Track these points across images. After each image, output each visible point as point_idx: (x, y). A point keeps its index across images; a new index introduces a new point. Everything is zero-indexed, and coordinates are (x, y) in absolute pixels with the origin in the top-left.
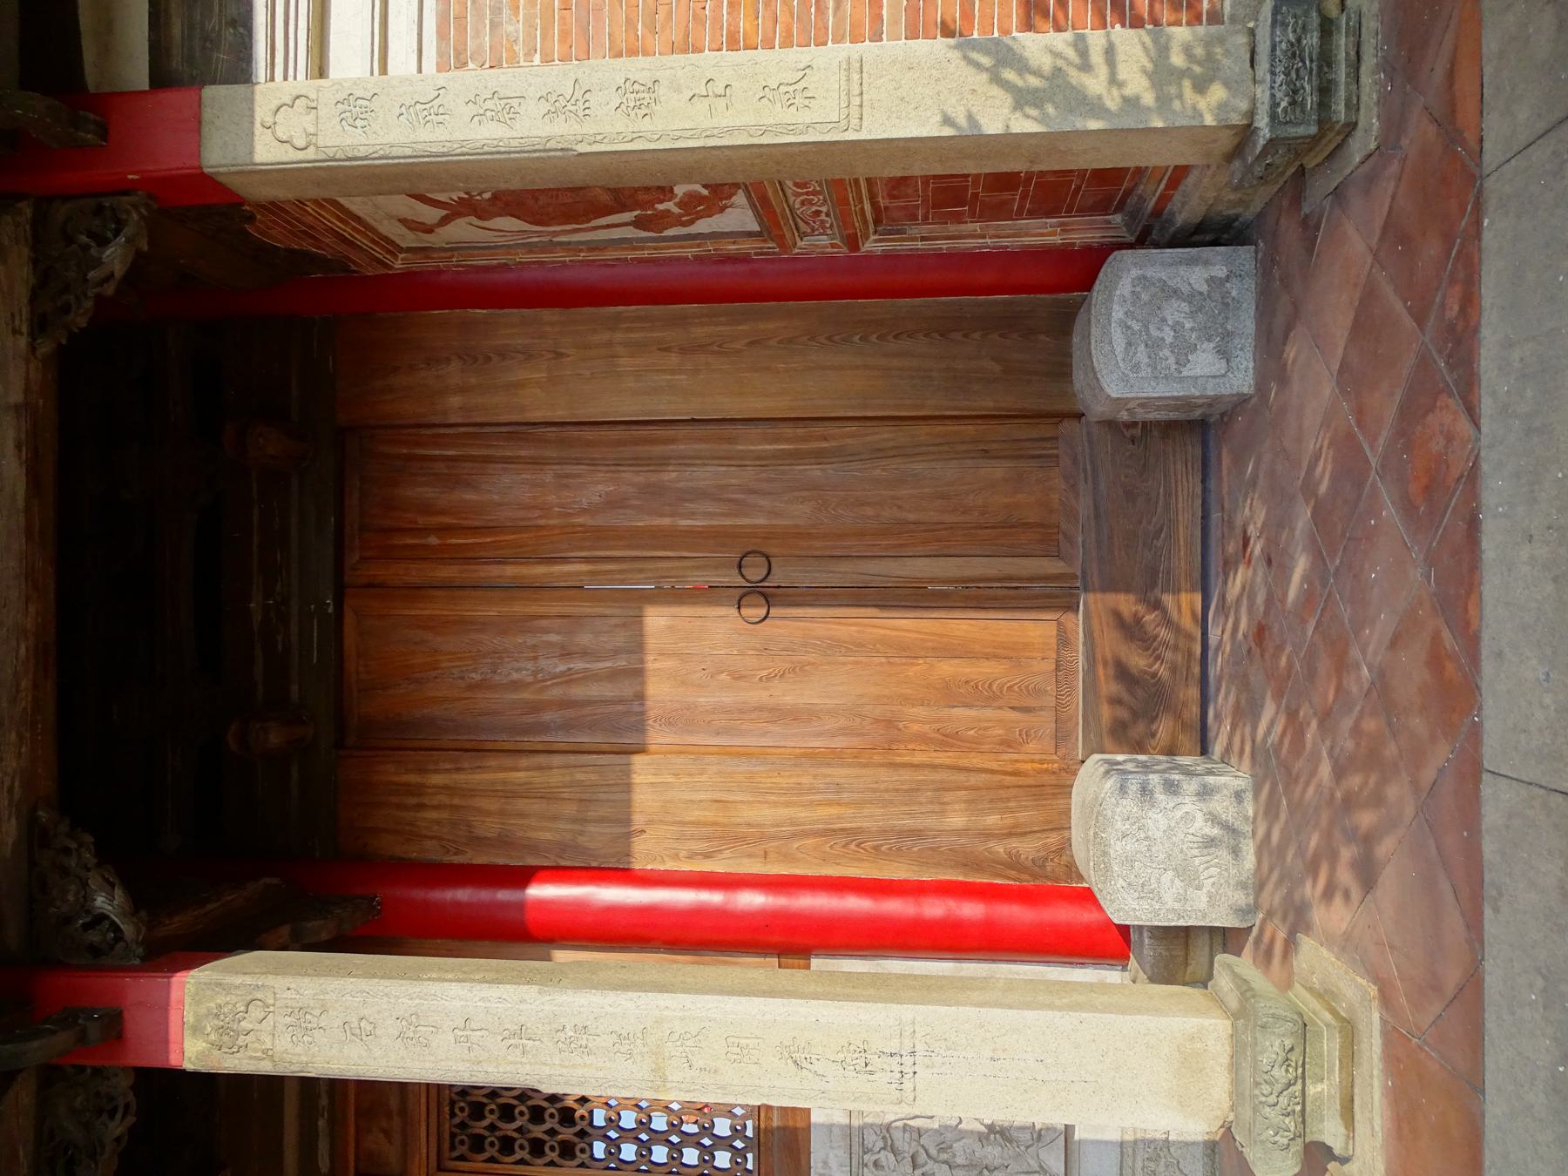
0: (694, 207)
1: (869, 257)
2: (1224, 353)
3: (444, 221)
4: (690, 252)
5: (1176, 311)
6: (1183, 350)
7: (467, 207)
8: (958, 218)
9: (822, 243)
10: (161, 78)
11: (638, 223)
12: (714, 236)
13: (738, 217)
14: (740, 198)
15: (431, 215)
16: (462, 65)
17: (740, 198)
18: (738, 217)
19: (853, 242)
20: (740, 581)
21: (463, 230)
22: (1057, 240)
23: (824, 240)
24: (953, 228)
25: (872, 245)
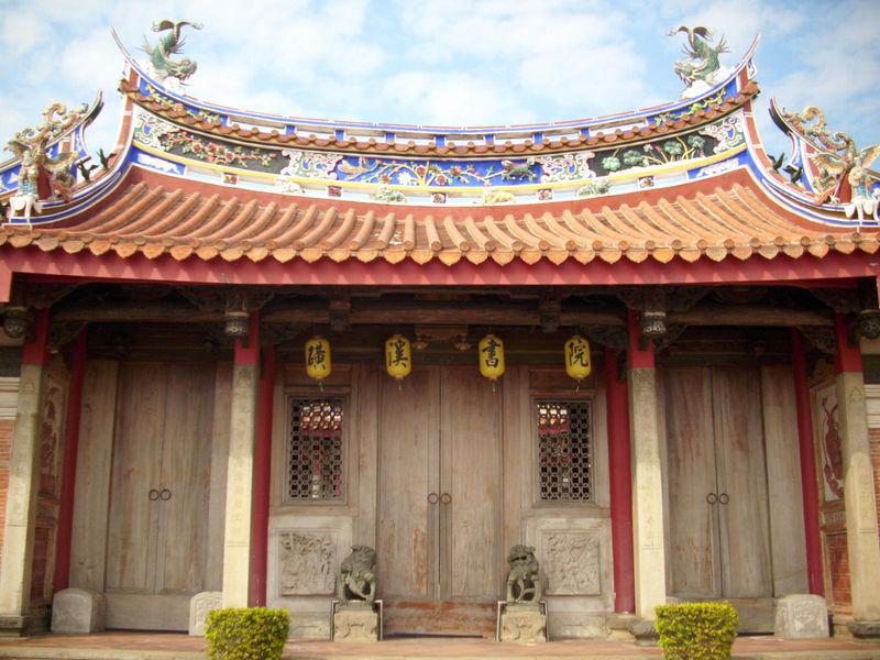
0: (834, 486)
1: (818, 533)
2: (801, 630)
3: (826, 411)
4: (818, 480)
5: (811, 618)
6: (802, 620)
7: (831, 422)
8: (831, 558)
9: (823, 520)
10: (865, 357)
11: (827, 466)
12: (823, 488)
13: (830, 495)
14: (836, 497)
15: (830, 409)
16: (870, 434)
17: (836, 497)
18: (830, 495)
19: (824, 528)
20: (720, 493)
21: (823, 416)
22: (826, 587)
23: (824, 522)
24: (828, 557)
25: (822, 534)
